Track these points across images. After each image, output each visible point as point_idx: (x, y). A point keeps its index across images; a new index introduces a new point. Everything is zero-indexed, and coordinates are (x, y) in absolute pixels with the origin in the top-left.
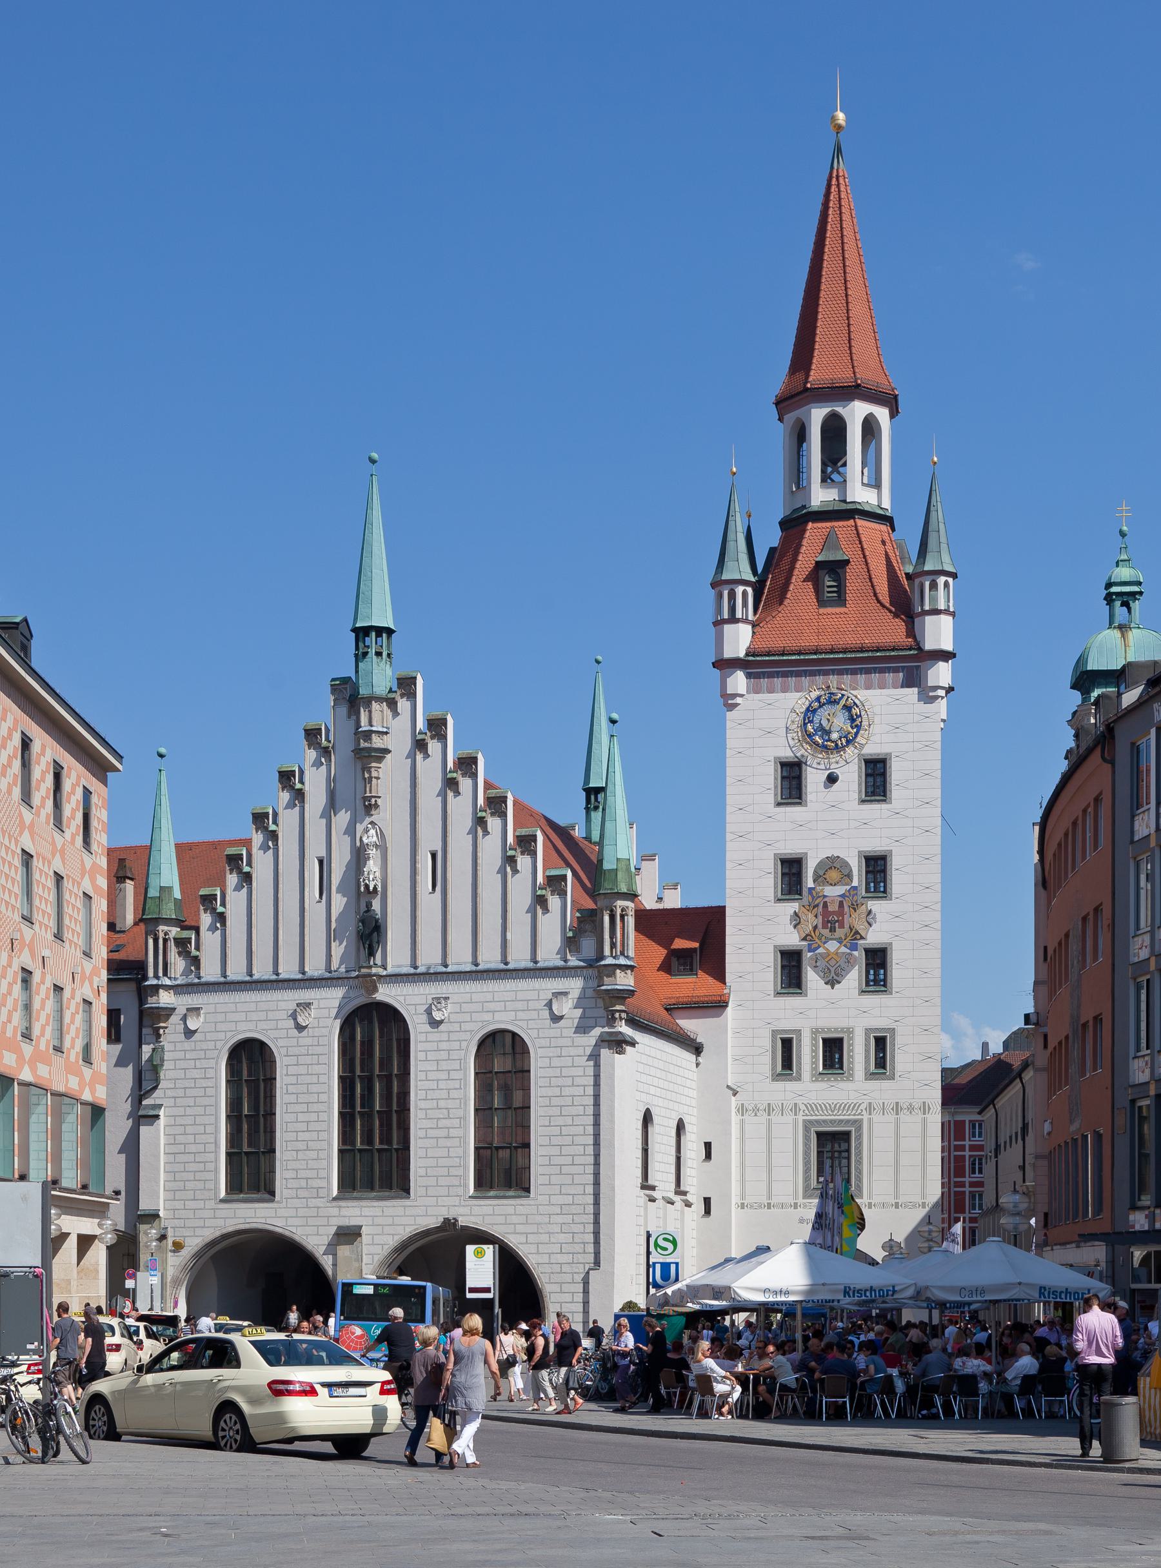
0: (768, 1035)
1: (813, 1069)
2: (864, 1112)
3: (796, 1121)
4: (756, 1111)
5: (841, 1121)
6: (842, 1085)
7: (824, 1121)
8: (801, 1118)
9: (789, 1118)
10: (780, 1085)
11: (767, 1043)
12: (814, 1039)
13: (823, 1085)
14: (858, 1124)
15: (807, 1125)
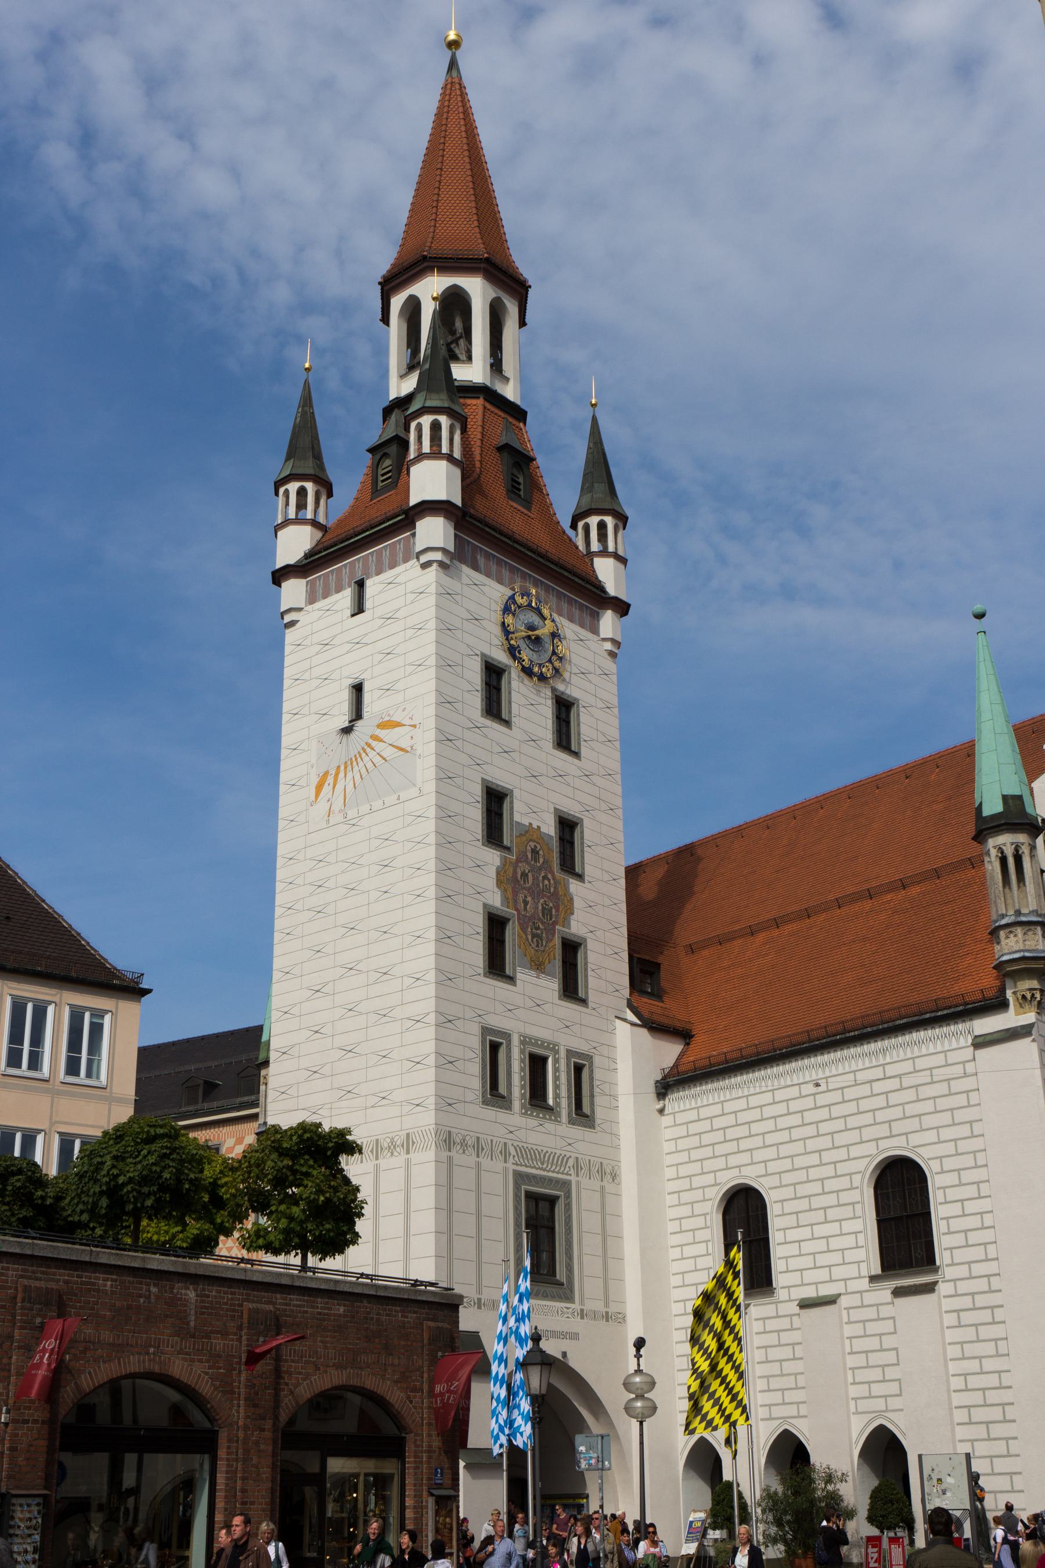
0: (476, 1029)
1: (523, 1096)
2: (572, 1172)
3: (506, 1169)
4: (464, 1145)
5: (550, 1180)
6: (550, 1126)
7: (535, 1176)
8: (511, 1167)
9: (498, 1165)
10: (491, 1113)
11: (475, 1042)
12: (522, 1052)
13: (532, 1122)
14: (566, 1185)
15: (520, 1178)
